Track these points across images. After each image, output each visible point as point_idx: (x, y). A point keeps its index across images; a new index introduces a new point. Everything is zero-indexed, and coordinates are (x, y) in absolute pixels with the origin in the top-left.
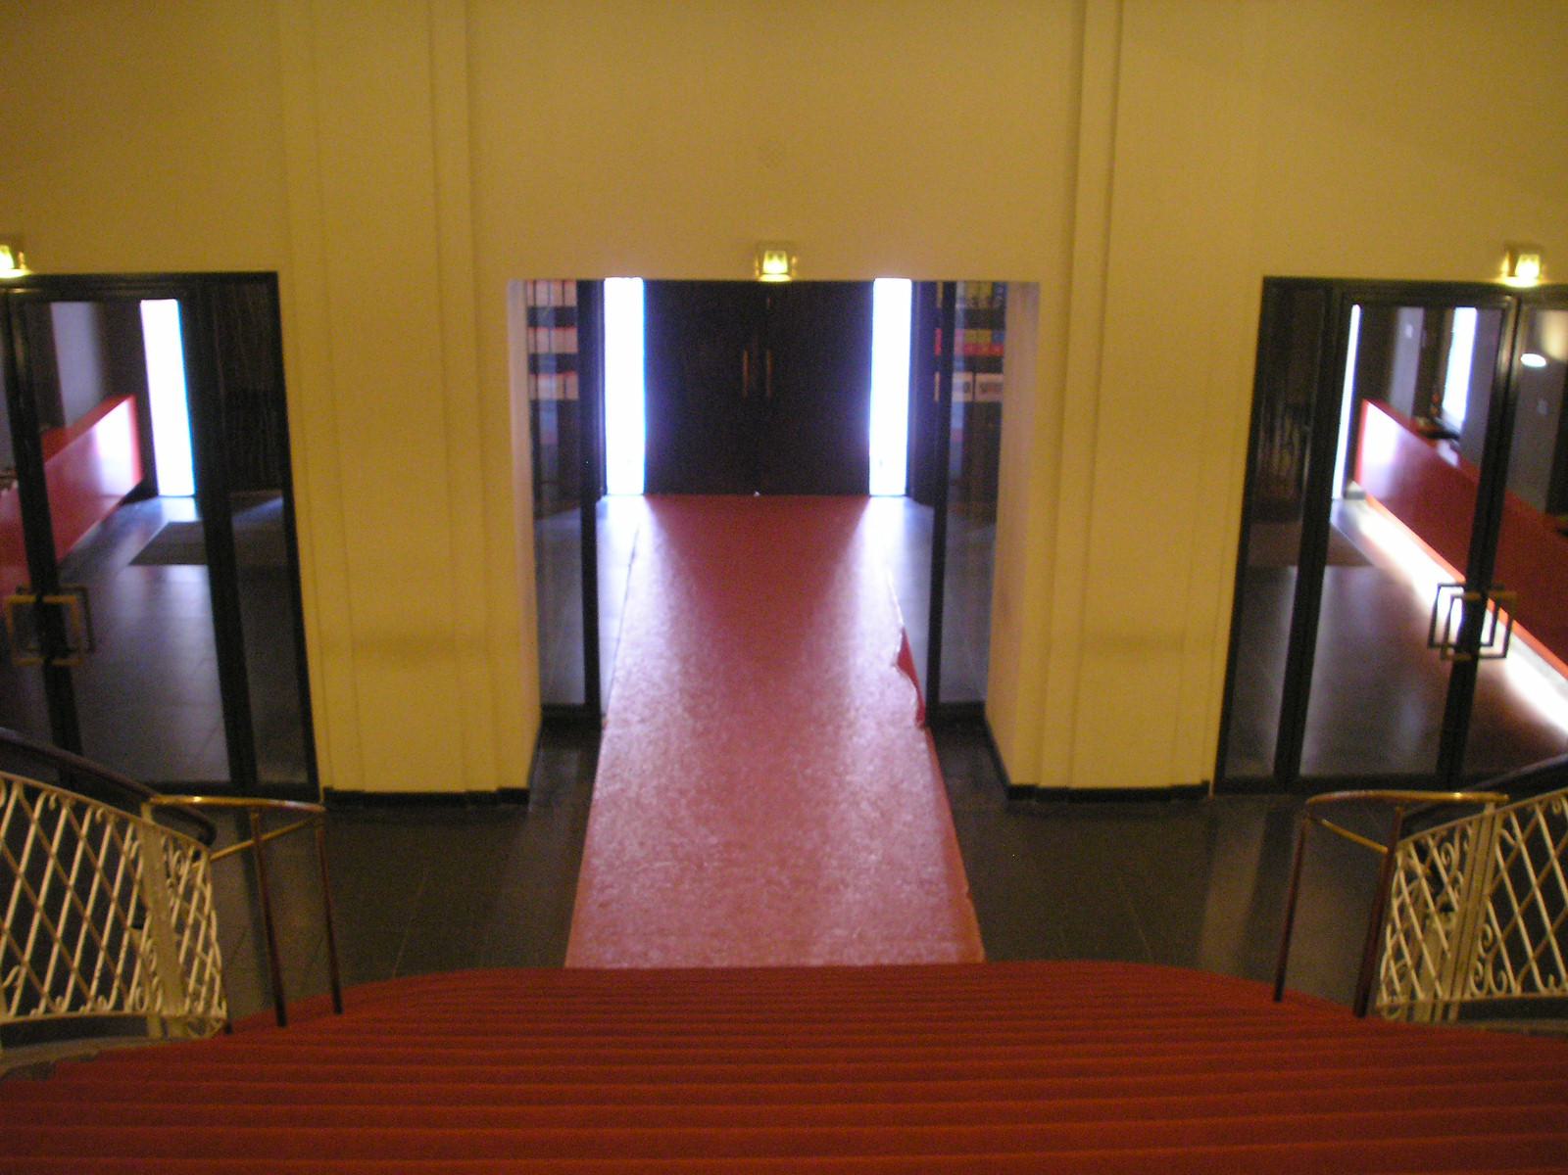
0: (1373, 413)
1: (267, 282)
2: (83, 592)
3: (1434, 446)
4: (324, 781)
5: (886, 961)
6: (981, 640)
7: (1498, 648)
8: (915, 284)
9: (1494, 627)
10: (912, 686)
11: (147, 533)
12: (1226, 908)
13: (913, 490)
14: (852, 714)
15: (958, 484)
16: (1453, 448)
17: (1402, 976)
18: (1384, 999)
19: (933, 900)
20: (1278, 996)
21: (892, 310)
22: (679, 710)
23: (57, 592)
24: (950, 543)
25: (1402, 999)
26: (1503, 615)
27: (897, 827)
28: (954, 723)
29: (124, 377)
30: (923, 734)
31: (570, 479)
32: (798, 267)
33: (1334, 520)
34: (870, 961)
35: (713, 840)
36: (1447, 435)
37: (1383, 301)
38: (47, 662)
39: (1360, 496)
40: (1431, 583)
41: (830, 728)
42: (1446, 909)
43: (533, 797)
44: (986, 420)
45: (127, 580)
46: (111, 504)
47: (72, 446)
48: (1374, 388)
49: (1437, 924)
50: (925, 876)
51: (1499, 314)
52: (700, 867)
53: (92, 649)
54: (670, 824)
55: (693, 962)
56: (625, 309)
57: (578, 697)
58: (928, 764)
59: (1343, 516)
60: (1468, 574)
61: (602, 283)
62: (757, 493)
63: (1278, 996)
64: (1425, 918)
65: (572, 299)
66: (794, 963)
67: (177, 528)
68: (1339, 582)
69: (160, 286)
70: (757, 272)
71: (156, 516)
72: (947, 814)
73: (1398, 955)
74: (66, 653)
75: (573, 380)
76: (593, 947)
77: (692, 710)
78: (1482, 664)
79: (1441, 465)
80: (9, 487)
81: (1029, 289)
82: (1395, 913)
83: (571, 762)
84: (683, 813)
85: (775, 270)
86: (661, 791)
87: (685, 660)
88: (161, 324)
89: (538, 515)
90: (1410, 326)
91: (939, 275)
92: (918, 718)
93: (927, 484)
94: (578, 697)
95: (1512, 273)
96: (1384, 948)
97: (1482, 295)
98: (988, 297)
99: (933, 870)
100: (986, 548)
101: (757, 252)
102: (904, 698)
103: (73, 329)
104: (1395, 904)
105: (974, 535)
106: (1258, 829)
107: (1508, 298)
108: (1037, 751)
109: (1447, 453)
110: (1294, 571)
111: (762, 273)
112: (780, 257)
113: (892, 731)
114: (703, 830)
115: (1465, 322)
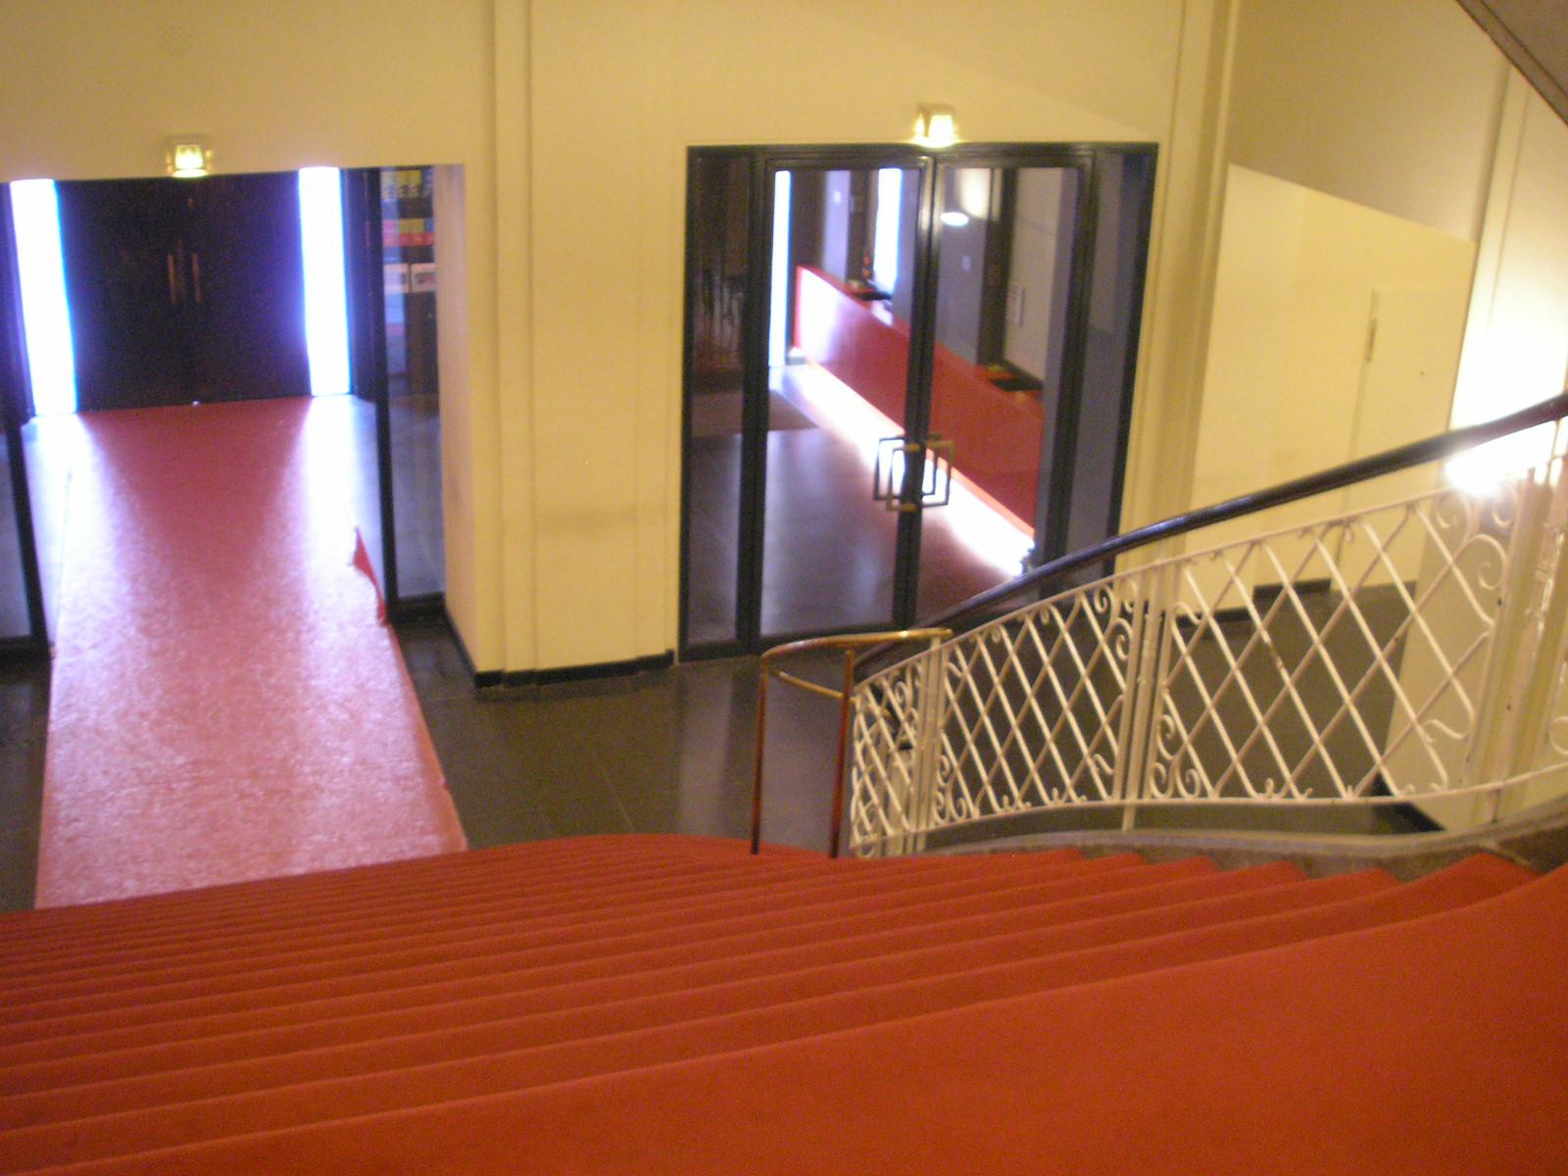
0: (807, 277)
3: (868, 307)
5: (368, 861)
6: (436, 533)
7: (940, 497)
8: (342, 172)
9: (936, 476)
10: (371, 584)
12: (701, 774)
13: (356, 387)
14: (311, 619)
15: (400, 379)
16: (887, 308)
17: (872, 816)
18: (857, 839)
19: (410, 796)
20: (755, 849)
22: (132, 631)
24: (395, 437)
25: (873, 838)
26: (943, 463)
27: (368, 727)
28: (417, 618)
30: (385, 631)
32: (213, 161)
33: (775, 383)
34: (352, 863)
35: (180, 760)
36: (881, 296)
37: (812, 166)
39: (802, 361)
40: (869, 437)
41: (290, 635)
42: (905, 747)
44: (422, 309)
48: (807, 252)
49: (899, 761)
50: (401, 773)
51: (916, 173)
52: (170, 789)
54: (133, 749)
55: (171, 887)
57: (24, 629)
58: (392, 660)
59: (787, 382)
60: (906, 423)
62: (196, 403)
63: (755, 849)
64: (887, 759)
66: (276, 874)
68: (788, 447)
72: (417, 709)
73: (866, 797)
76: (63, 885)
77: (146, 630)
78: (927, 513)
79: (875, 325)
81: (454, 171)
82: (859, 757)
84: (148, 736)
85: (189, 165)
86: (122, 716)
87: (134, 579)
90: (837, 189)
92: (379, 616)
93: (371, 380)
94: (24, 629)
95: (926, 134)
96: (851, 792)
97: (900, 155)
98: (417, 186)
99: (408, 766)
100: (431, 441)
102: (363, 597)
104: (858, 747)
105: (420, 428)
106: (726, 691)
107: (924, 158)
108: (501, 636)
109: (882, 313)
110: (739, 437)
111: (175, 170)
113: (353, 631)
114: (170, 752)
115: (889, 182)
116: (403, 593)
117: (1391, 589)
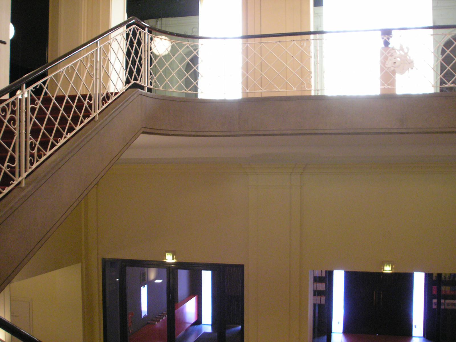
11: (198, 335)
21: (419, 281)
29: (195, 291)
46: (188, 325)
47: (180, 308)
56: (339, 278)
61: (333, 271)
62: (377, 334)
65: (324, 275)
67: (206, 334)
70: (382, 270)
71: (201, 330)
75: (323, 298)
85: (388, 269)
88: (207, 276)
89: (314, 337)
103: (183, 276)
111: (384, 270)
112: (389, 265)
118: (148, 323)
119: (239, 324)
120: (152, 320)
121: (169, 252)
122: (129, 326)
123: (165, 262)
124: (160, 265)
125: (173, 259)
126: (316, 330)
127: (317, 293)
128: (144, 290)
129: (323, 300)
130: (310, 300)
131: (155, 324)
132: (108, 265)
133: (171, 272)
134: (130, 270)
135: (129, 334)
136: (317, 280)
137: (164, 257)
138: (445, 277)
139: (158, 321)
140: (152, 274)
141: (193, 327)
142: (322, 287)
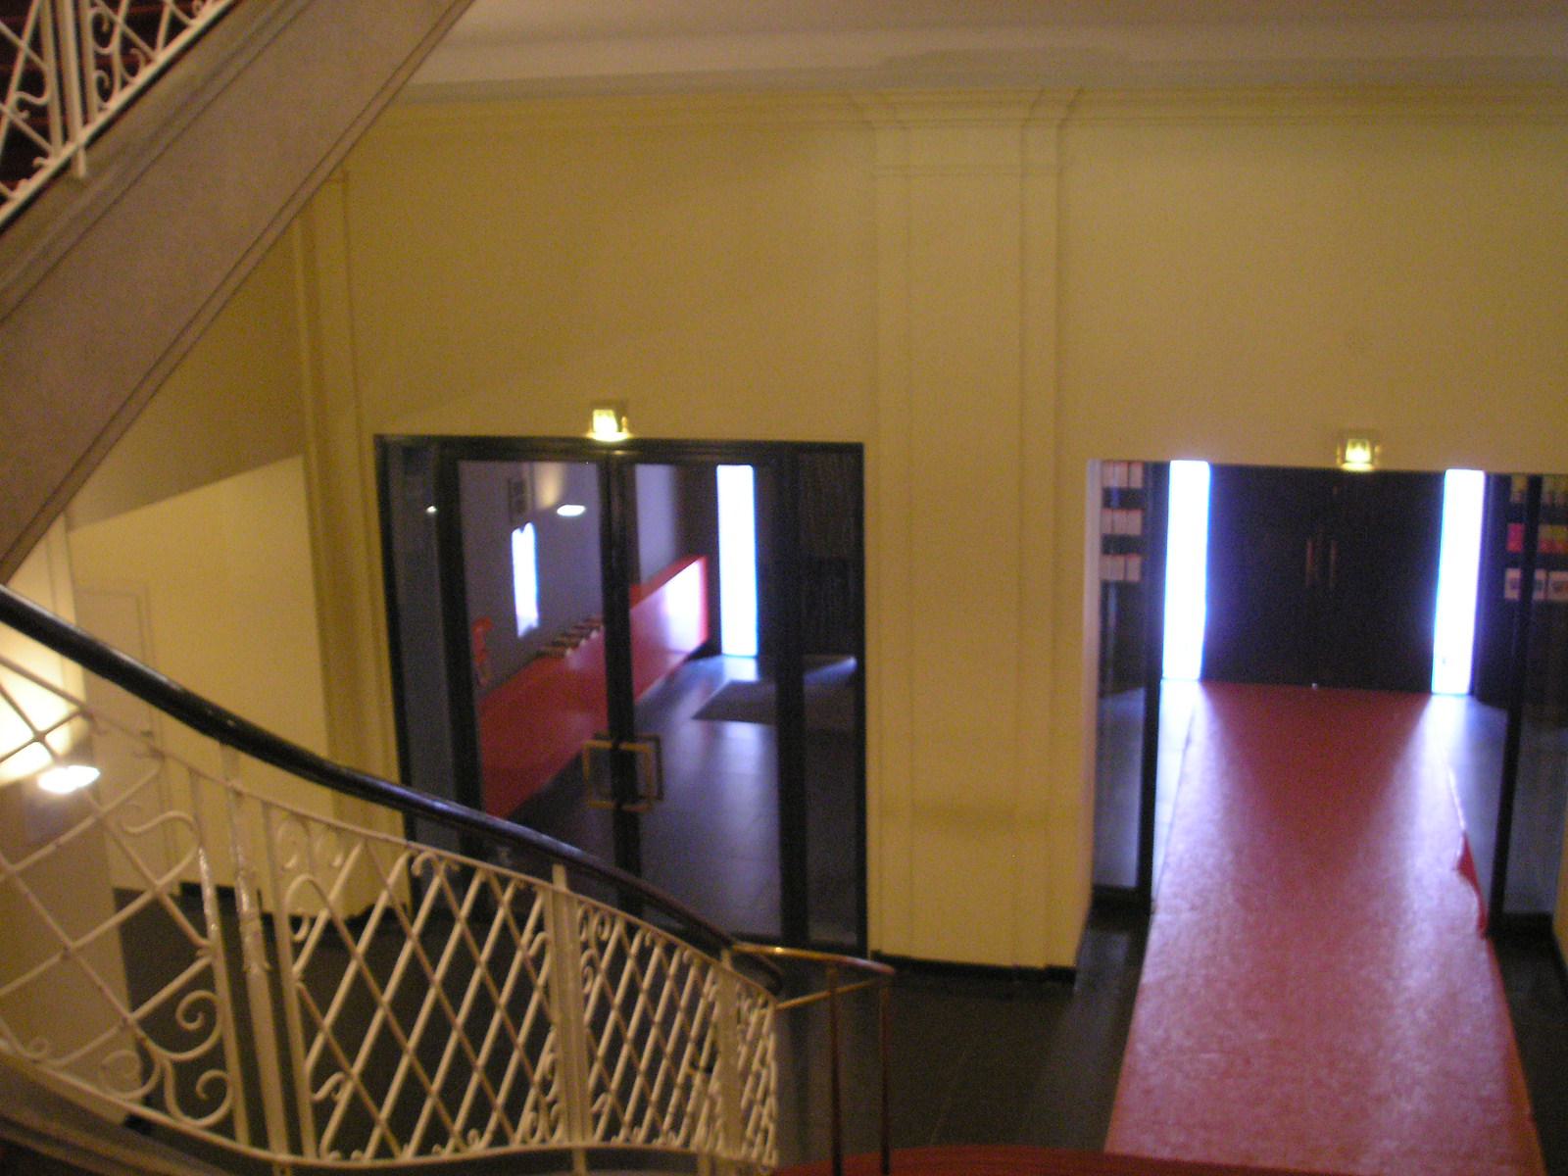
1: (850, 456)
2: (657, 741)
4: (874, 943)
8: (1488, 478)
10: (1473, 893)
13: (1476, 688)
14: (1410, 917)
23: (633, 739)
29: (697, 539)
30: (1484, 943)
31: (1130, 661)
32: (1382, 457)
38: (619, 806)
41: (1385, 931)
43: (1079, 977)
45: (686, 732)
46: (675, 660)
47: (648, 601)
50: (1484, 1093)
53: (660, 796)
56: (1190, 490)
57: (1129, 879)
58: (1488, 975)
62: (1314, 685)
65: (1137, 482)
67: (738, 687)
69: (737, 453)
71: (718, 674)
72: (1508, 1030)
74: (636, 798)
76: (1138, 1129)
80: (587, 637)
83: (1119, 945)
84: (1231, 1005)
85: (1358, 459)
86: (1209, 981)
88: (736, 489)
89: (1102, 694)
91: (1504, 469)
92: (1480, 925)
94: (1129, 879)
99: (1491, 1088)
101: (1341, 440)
102: (1467, 904)
111: (1344, 461)
112: (1364, 445)
116: (1510, 906)
117: (126, 929)
118: (540, 655)
119: (846, 653)
120: (555, 644)
121: (604, 405)
122: (476, 664)
123: (590, 441)
124: (575, 450)
125: (620, 430)
126: (1110, 671)
127: (1114, 545)
128: (524, 544)
129: (1131, 569)
130: (1092, 570)
131: (563, 655)
132: (396, 459)
133: (613, 475)
134: (472, 472)
135: (476, 692)
136: (1118, 499)
137: (587, 422)
138: (1553, 498)
139: (575, 646)
140: (548, 484)
141: (692, 664)
142: (1130, 523)
